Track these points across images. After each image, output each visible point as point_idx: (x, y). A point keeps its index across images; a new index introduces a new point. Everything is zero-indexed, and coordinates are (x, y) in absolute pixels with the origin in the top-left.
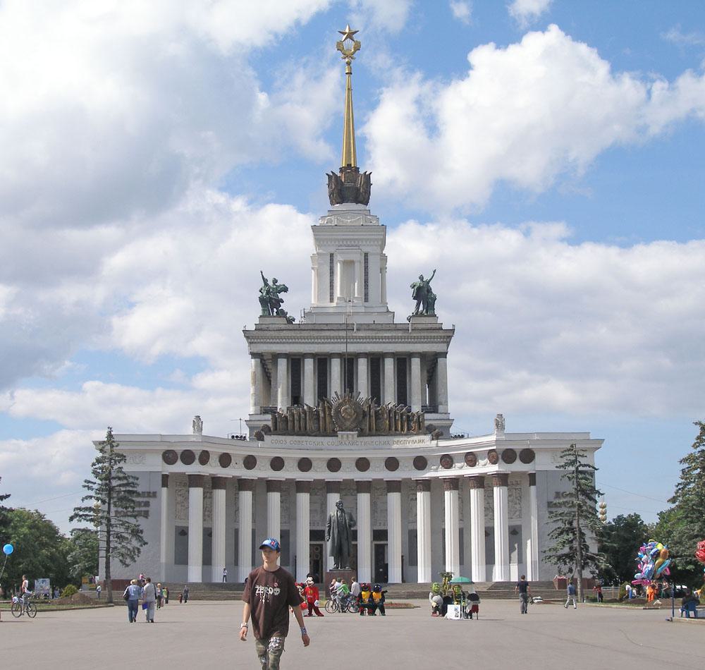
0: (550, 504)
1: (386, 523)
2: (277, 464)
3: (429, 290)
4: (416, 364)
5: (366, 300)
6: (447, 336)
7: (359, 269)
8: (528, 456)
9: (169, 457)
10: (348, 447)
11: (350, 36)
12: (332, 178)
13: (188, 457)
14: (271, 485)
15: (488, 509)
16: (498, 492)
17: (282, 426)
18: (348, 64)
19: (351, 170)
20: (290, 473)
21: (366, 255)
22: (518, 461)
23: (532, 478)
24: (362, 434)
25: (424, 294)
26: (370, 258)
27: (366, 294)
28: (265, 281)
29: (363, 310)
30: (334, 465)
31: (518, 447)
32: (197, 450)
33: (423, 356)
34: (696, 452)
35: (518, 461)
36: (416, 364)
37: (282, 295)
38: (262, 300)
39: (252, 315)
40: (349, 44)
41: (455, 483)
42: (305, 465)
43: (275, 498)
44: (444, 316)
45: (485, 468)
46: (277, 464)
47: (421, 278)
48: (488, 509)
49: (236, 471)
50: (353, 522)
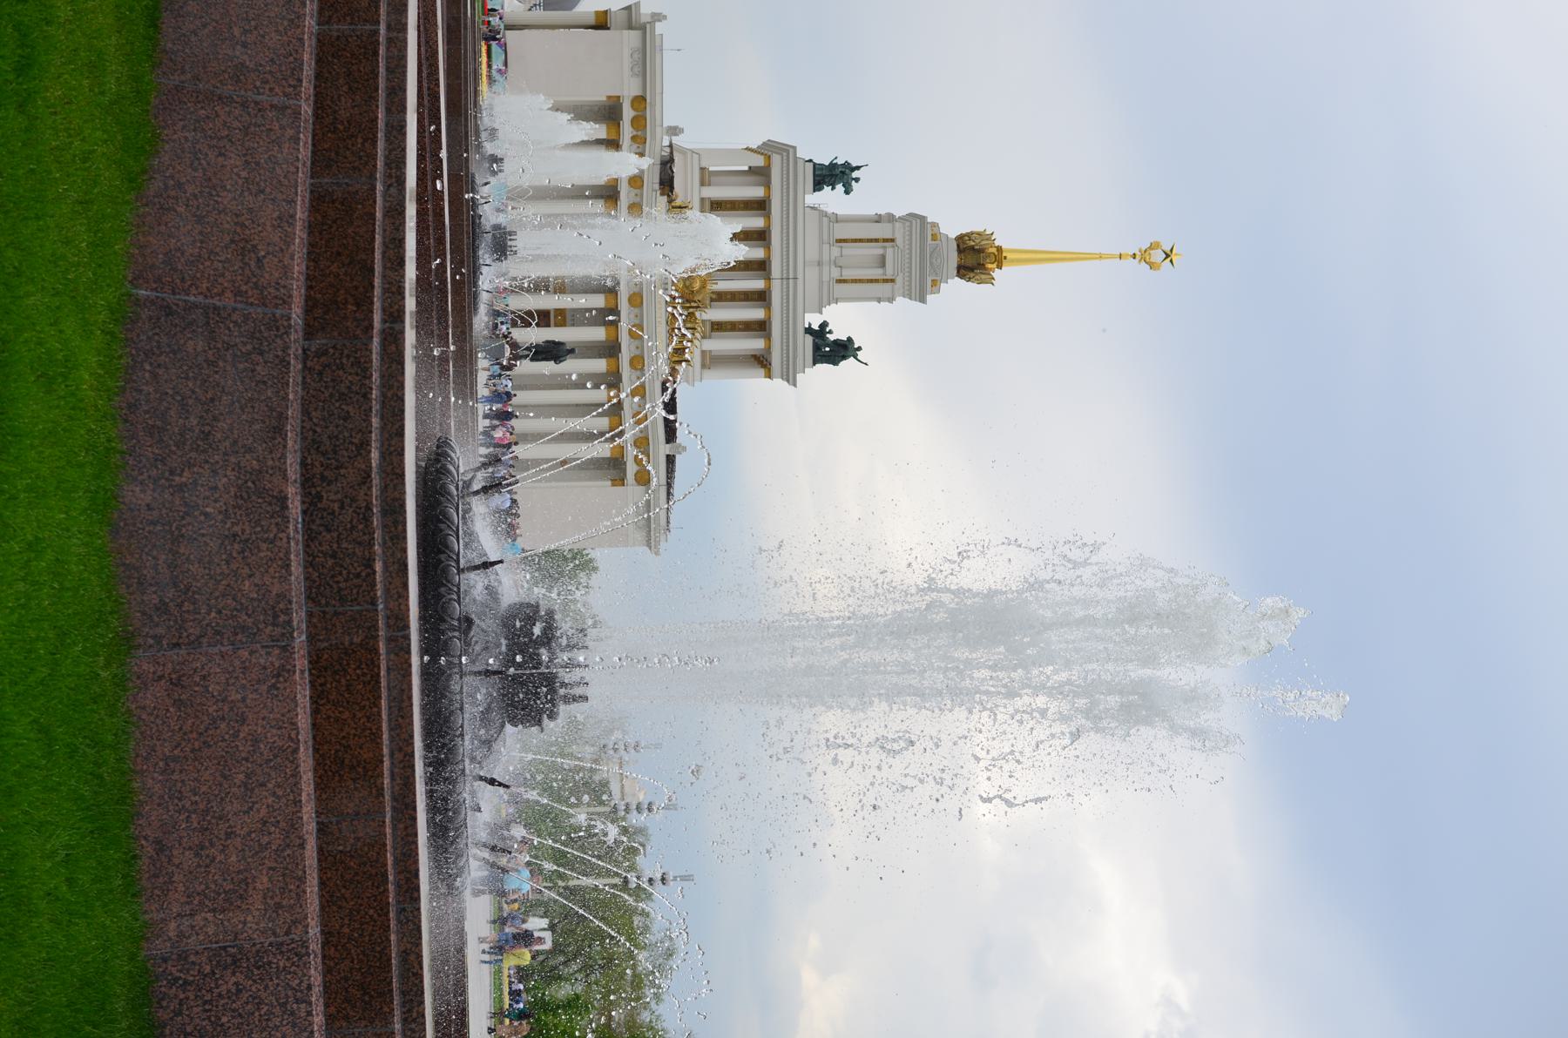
3: (844, 358)
4: (757, 344)
5: (839, 281)
7: (876, 273)
9: (640, 101)
13: (639, 122)
15: (589, 437)
18: (1134, 256)
19: (999, 258)
21: (892, 281)
26: (889, 285)
27: (845, 281)
28: (858, 168)
29: (826, 278)
33: (768, 349)
37: (840, 188)
38: (833, 166)
40: (1158, 256)
47: (859, 349)
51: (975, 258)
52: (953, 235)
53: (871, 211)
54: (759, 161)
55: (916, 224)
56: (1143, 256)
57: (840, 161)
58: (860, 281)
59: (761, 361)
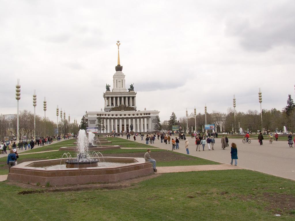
0: (152, 121)
1: (128, 123)
2: (113, 115)
4: (131, 98)
7: (121, 82)
8: (149, 114)
9: (98, 115)
10: (123, 112)
11: (118, 42)
13: (101, 115)
16: (145, 119)
17: (113, 109)
19: (119, 65)
20: (114, 116)
22: (148, 115)
23: (150, 117)
24: (125, 110)
25: (132, 88)
26: (123, 80)
30: (121, 115)
32: (102, 113)
33: (132, 97)
34: (172, 116)
35: (148, 115)
36: (131, 98)
37: (109, 87)
38: (106, 88)
39: (105, 90)
40: (118, 44)
41: (139, 118)
42: (117, 115)
43: (112, 120)
44: (135, 90)
45: (143, 115)
46: (113, 115)
48: (144, 121)
49: (107, 116)
50: (113, 122)
51: (119, 68)
52: (116, 72)
53: (113, 83)
54: (106, 98)
55: (115, 77)
56: (118, 45)
57: (106, 87)
58: (122, 85)
59: (133, 98)
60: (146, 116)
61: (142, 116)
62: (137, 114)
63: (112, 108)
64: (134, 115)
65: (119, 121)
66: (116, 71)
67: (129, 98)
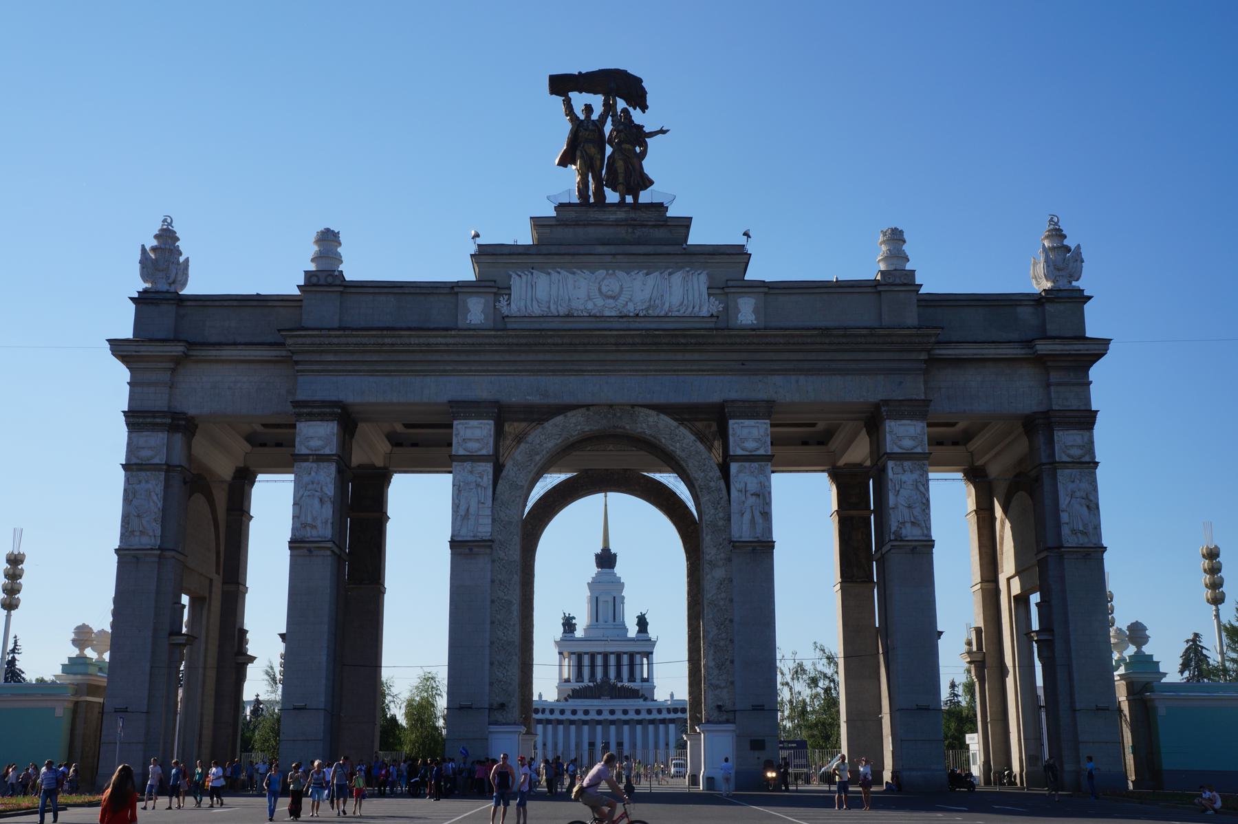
2: (574, 712)
6: (653, 644)
10: (606, 704)
12: (597, 556)
14: (572, 722)
25: (642, 623)
31: (679, 707)
36: (638, 657)
38: (564, 625)
41: (652, 722)
44: (652, 632)
45: (665, 715)
46: (574, 712)
48: (667, 733)
49: (557, 716)
60: (672, 716)
61: (660, 717)
62: (649, 712)
63: (574, 691)
64: (638, 712)
65: (592, 733)
66: (598, 566)
67: (632, 656)
